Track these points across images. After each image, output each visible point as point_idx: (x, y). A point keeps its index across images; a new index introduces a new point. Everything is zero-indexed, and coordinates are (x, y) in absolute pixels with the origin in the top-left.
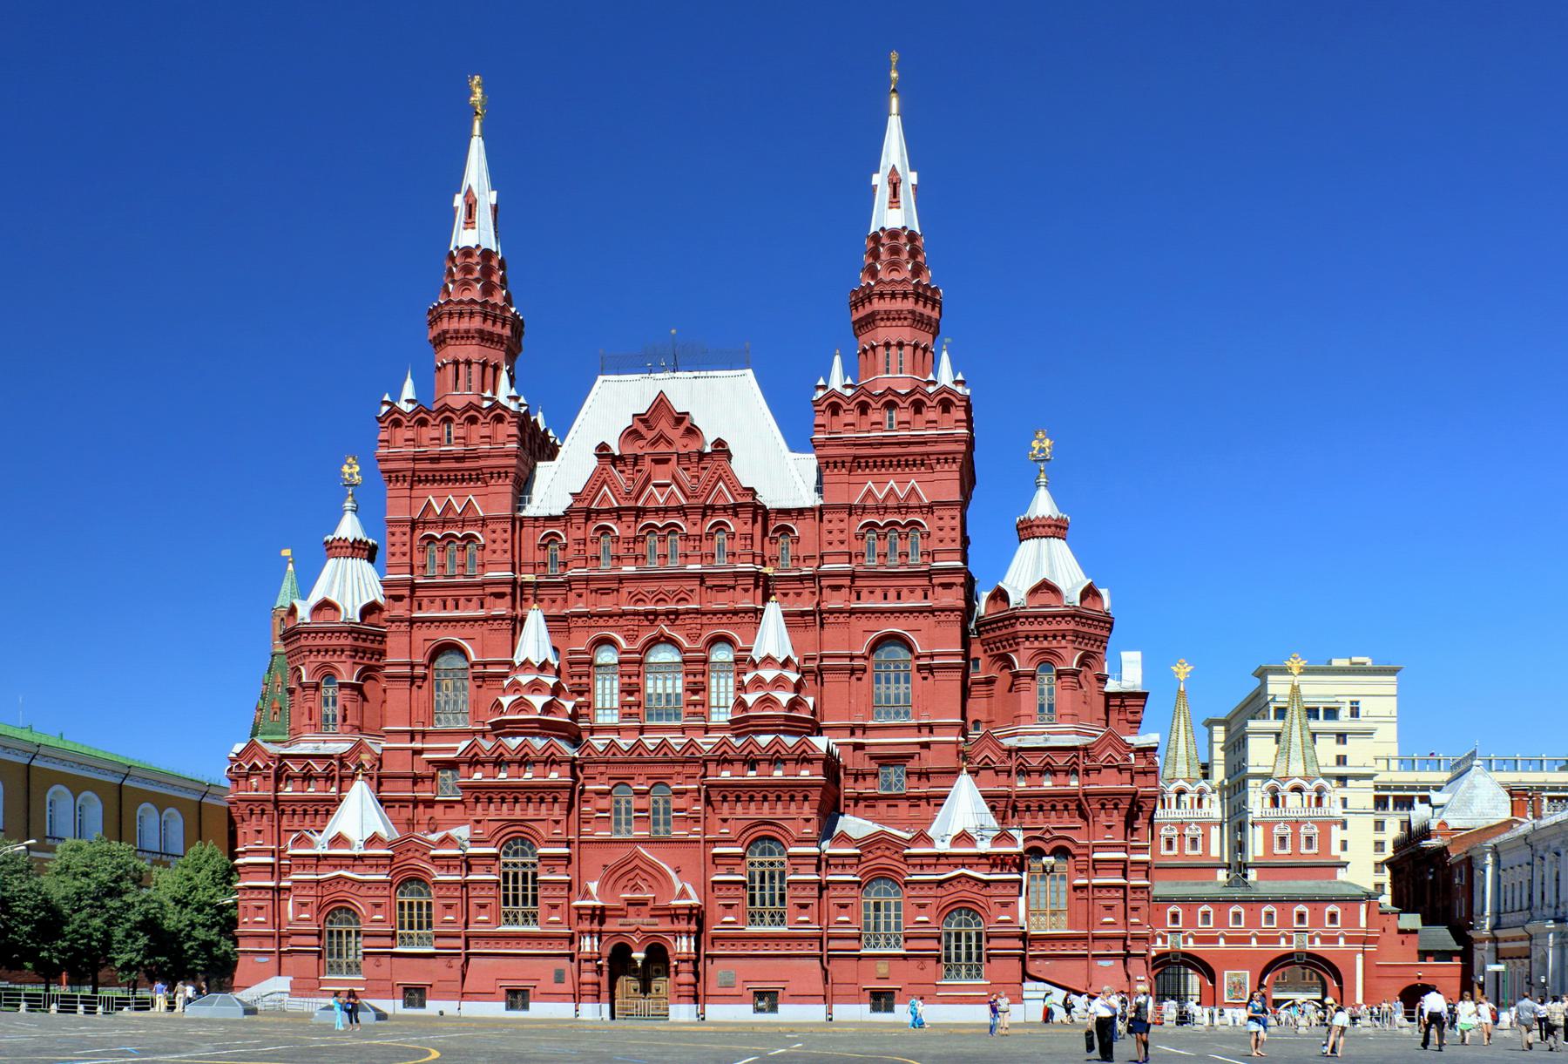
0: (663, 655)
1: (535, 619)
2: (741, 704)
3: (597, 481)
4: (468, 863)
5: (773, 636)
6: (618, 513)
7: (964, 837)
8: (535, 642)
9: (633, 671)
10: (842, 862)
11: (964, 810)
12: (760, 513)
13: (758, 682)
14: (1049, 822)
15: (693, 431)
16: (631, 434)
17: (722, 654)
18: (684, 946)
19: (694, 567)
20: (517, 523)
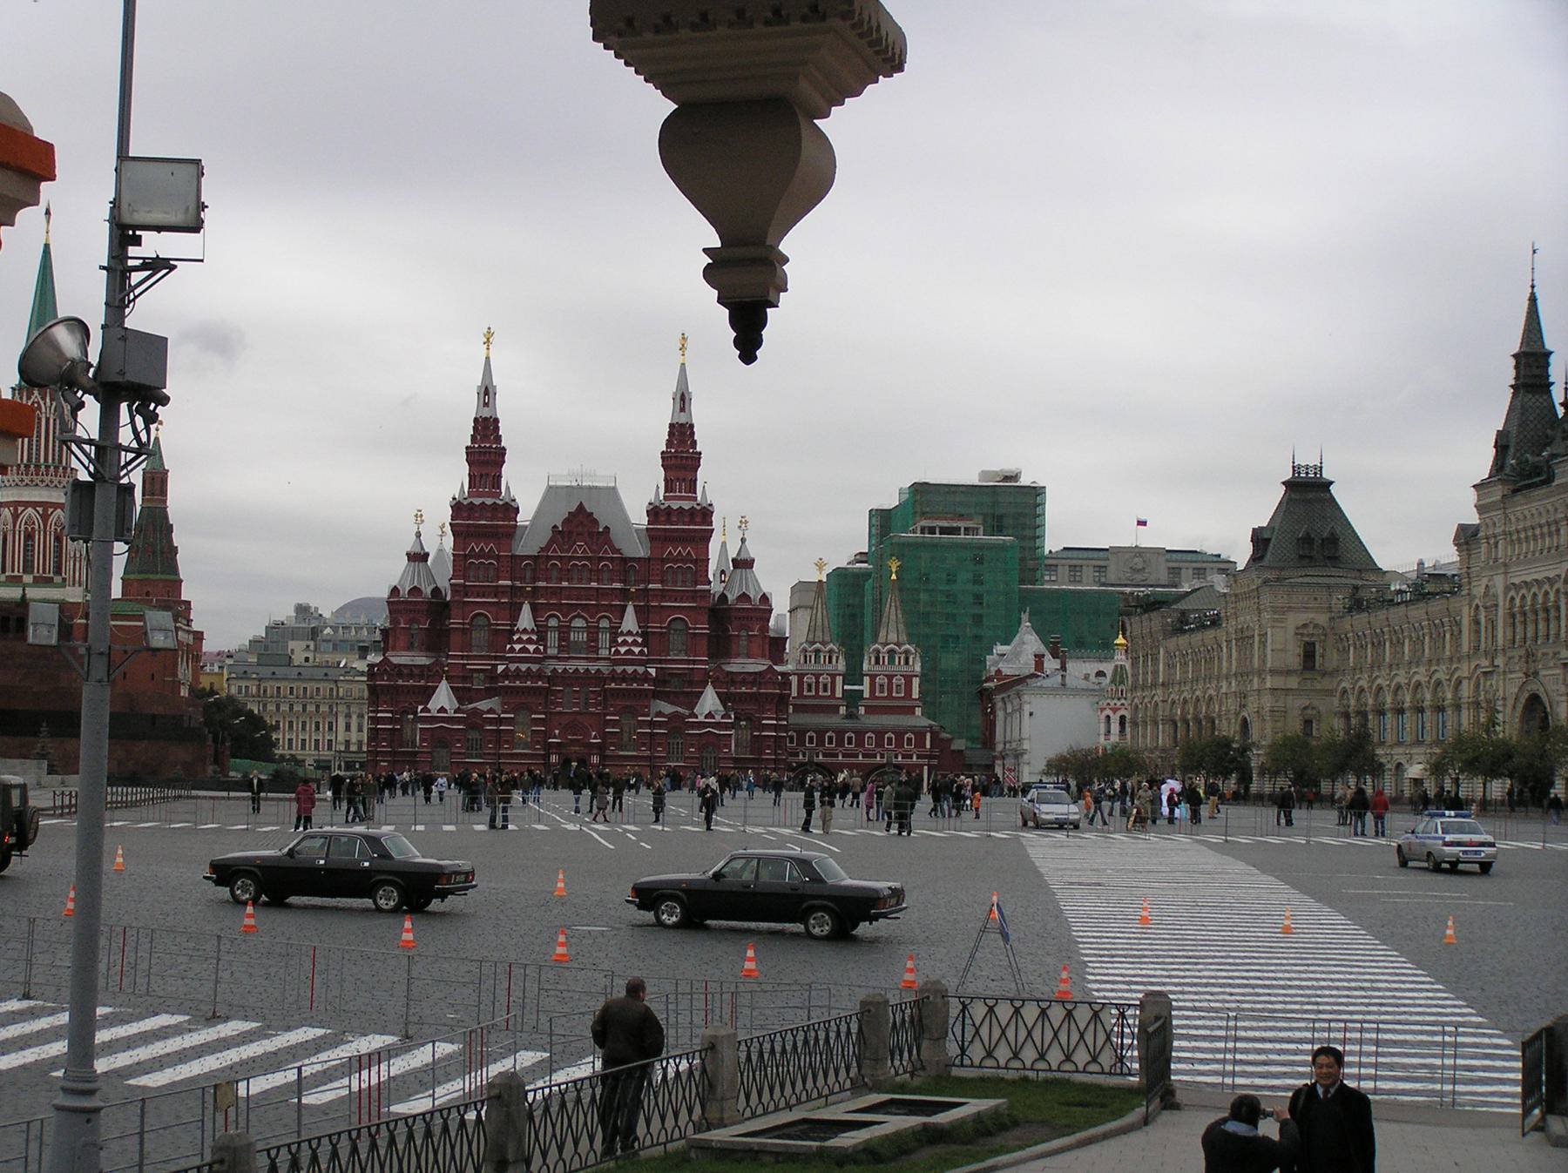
0: (578, 623)
1: (526, 608)
2: (617, 653)
3: (551, 541)
4: (500, 721)
5: (630, 622)
6: (560, 558)
7: (710, 715)
8: (526, 620)
9: (564, 631)
10: (660, 725)
11: (709, 701)
12: (625, 560)
13: (625, 643)
14: (750, 707)
15: (596, 522)
16: (566, 521)
17: (604, 624)
18: (595, 759)
19: (594, 584)
20: (513, 557)
